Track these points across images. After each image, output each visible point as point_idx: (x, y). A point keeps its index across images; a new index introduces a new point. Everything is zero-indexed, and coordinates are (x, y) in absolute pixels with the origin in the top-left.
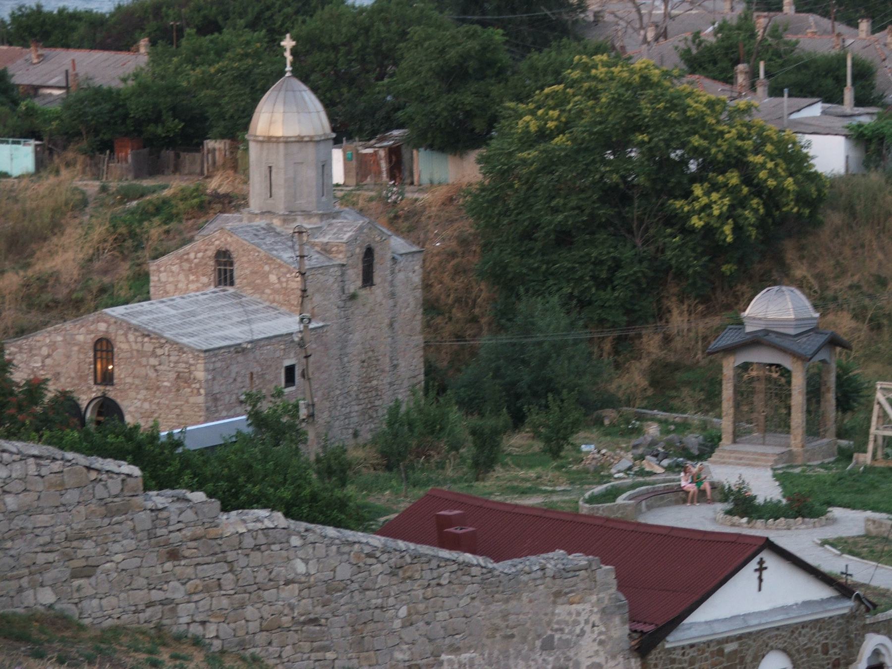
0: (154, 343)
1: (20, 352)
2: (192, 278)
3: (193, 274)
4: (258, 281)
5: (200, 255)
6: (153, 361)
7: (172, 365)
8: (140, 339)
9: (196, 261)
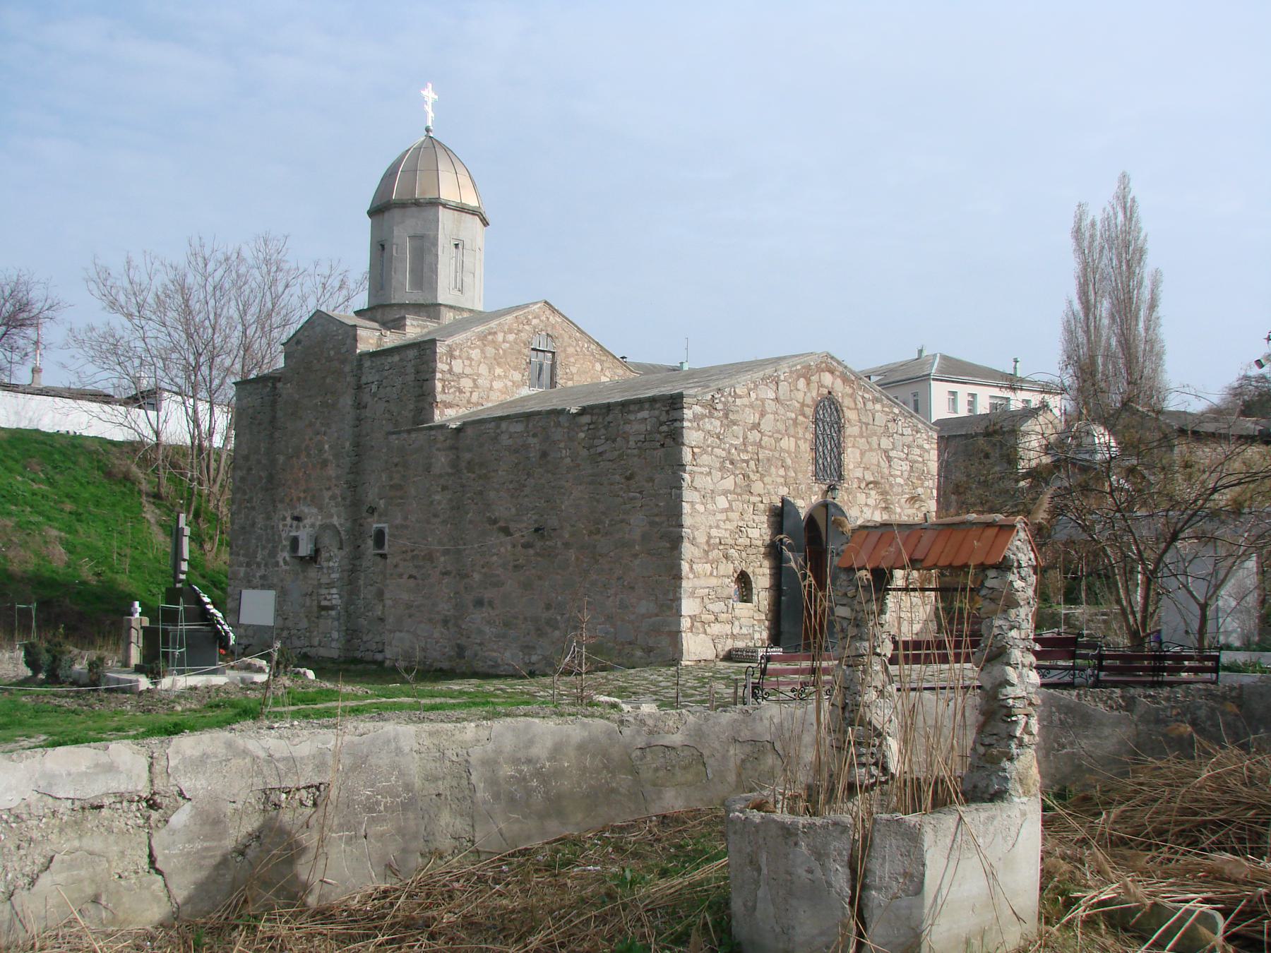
1: (711, 416)
2: (498, 371)
5: (511, 337)
6: (885, 443)
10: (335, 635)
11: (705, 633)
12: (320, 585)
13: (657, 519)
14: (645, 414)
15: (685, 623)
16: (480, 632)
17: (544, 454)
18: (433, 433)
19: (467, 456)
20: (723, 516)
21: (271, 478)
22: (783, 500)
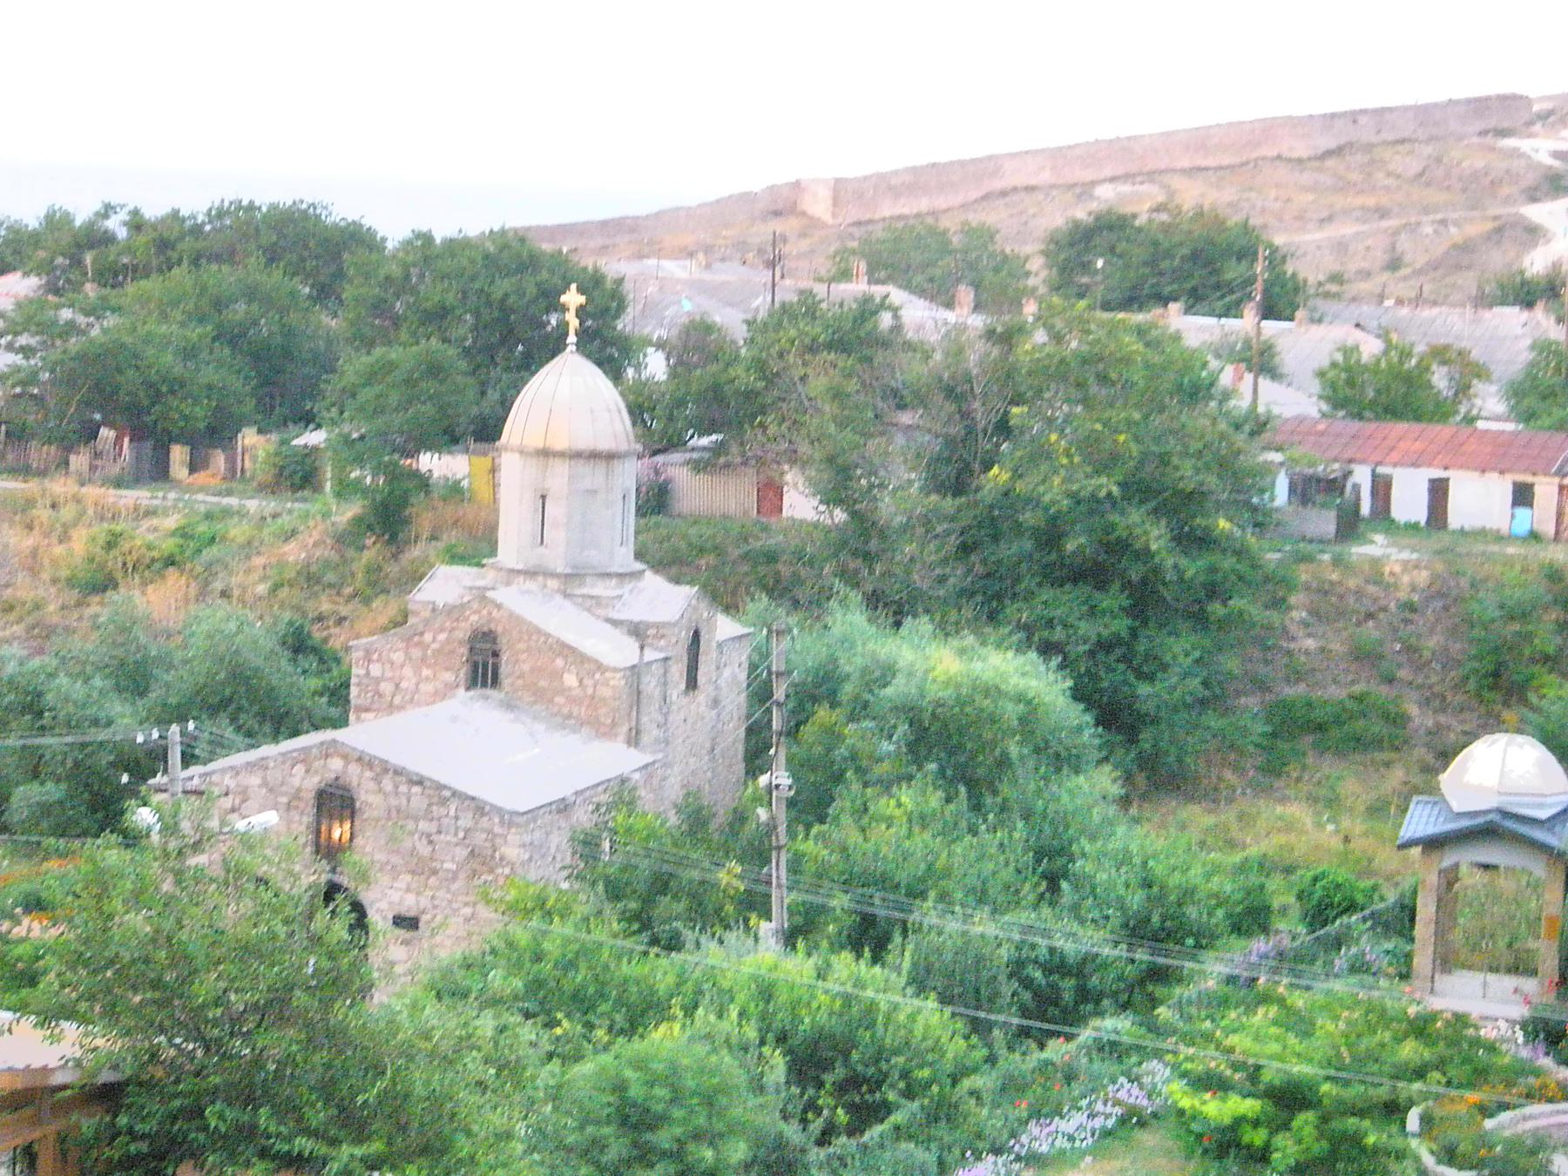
0: (429, 796)
2: (426, 672)
3: (428, 667)
4: (543, 683)
5: (442, 637)
6: (423, 826)
7: (461, 835)
8: (403, 788)
9: (435, 646)
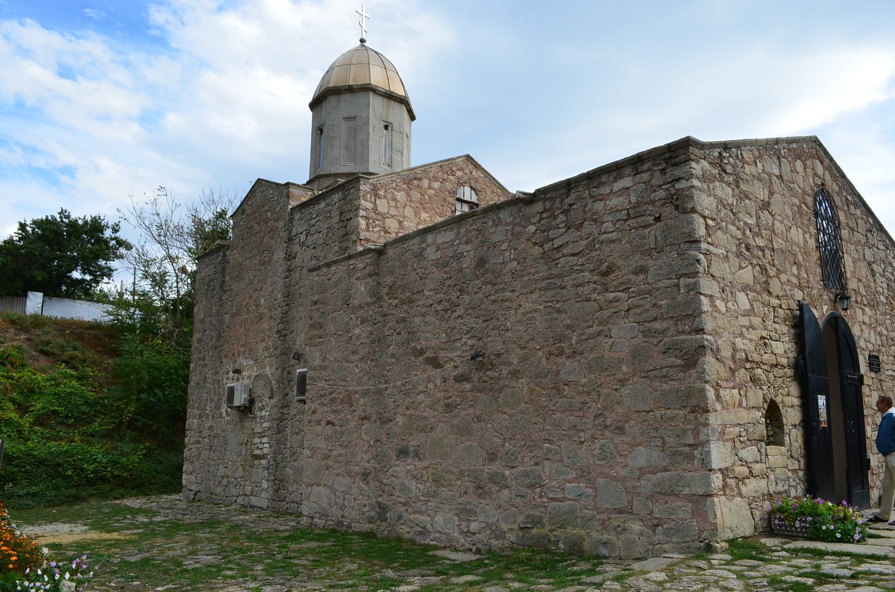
5: (436, 185)
10: (265, 484)
11: (740, 494)
12: (254, 435)
13: (657, 325)
14: (626, 182)
15: (717, 480)
16: (404, 488)
17: (481, 262)
18: (352, 261)
19: (389, 280)
20: (745, 321)
21: (219, 337)
22: (801, 306)
